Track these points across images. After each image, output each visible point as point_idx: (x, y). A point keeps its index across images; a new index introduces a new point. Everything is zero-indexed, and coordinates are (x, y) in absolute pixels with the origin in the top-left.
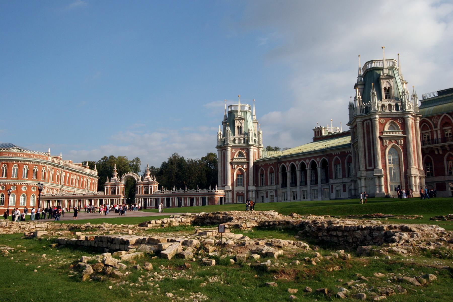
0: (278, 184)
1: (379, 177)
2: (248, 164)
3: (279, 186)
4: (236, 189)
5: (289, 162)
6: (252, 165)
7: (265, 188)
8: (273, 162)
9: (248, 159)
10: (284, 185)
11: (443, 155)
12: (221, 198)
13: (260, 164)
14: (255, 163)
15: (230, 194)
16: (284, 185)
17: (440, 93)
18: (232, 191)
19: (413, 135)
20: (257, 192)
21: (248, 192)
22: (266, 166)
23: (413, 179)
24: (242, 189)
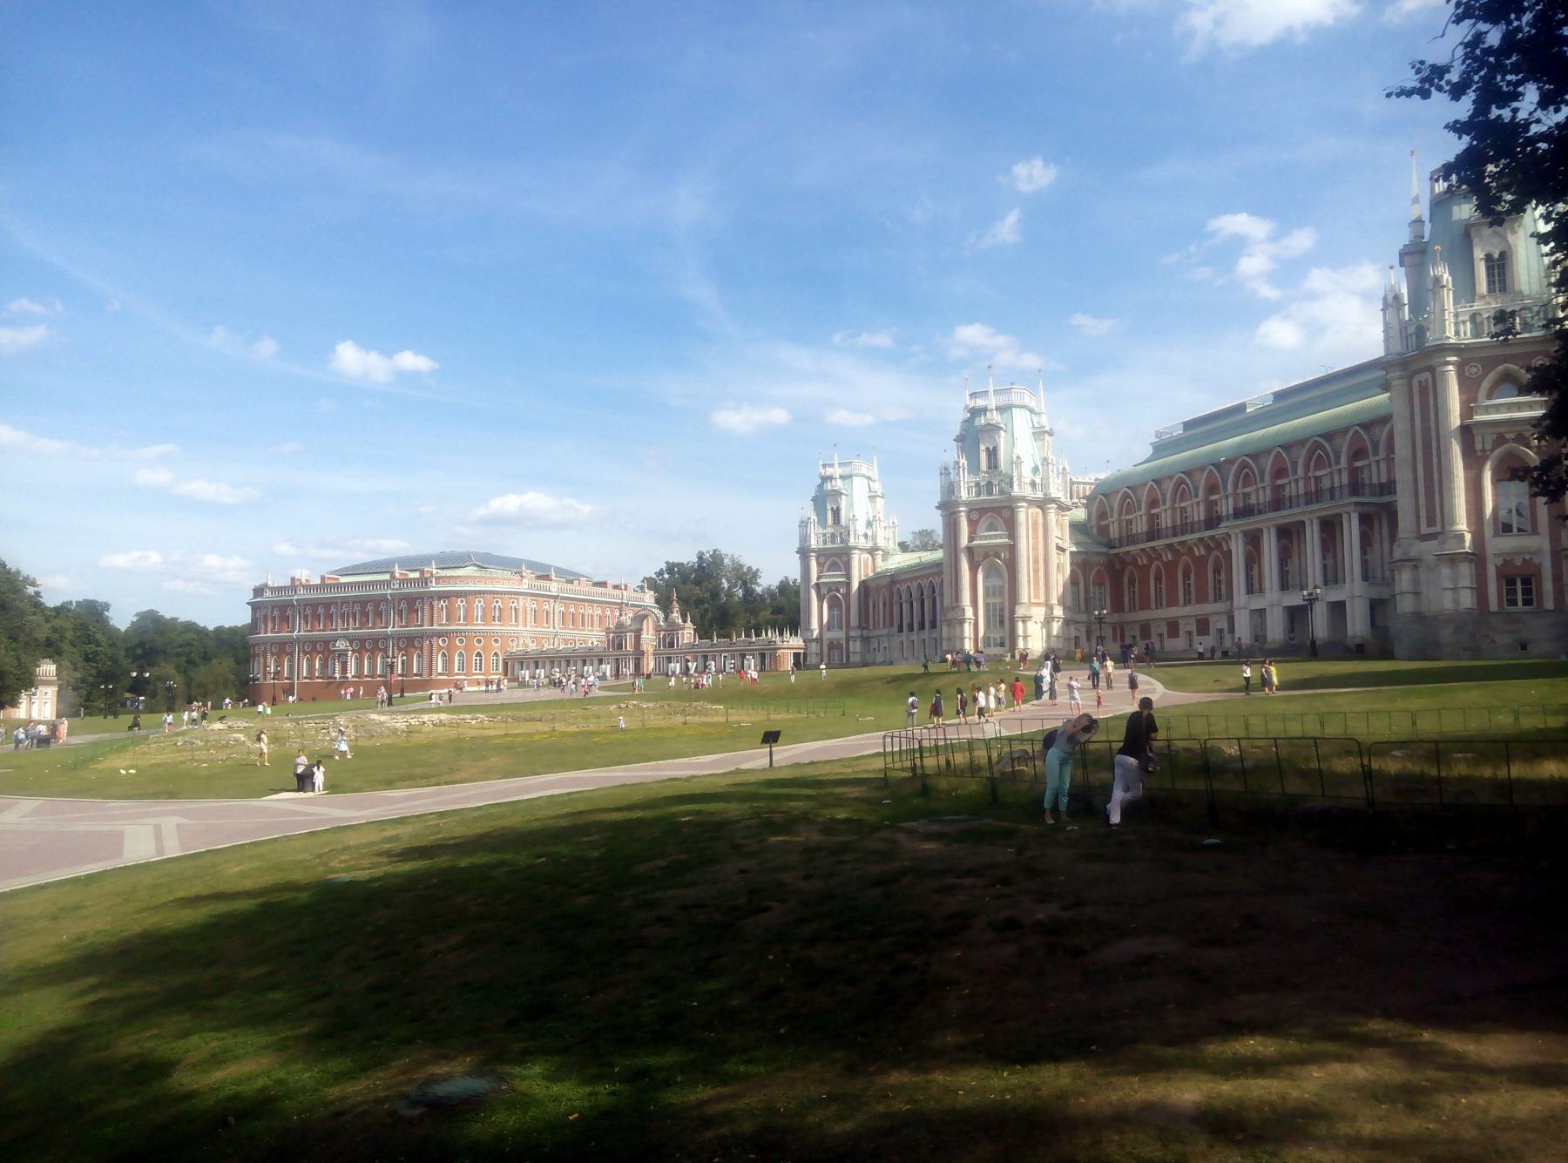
0: (892, 625)
1: (962, 622)
2: (848, 585)
3: (895, 628)
4: (827, 635)
5: (905, 581)
6: (855, 586)
7: (878, 632)
8: (885, 582)
9: (848, 576)
10: (901, 630)
11: (1149, 566)
12: (796, 656)
13: (872, 585)
14: (863, 584)
15: (814, 647)
16: (901, 630)
17: (1188, 425)
18: (819, 640)
19: (1036, 538)
20: (865, 640)
21: (848, 638)
22: (879, 588)
23: (1020, 625)
24: (839, 635)
